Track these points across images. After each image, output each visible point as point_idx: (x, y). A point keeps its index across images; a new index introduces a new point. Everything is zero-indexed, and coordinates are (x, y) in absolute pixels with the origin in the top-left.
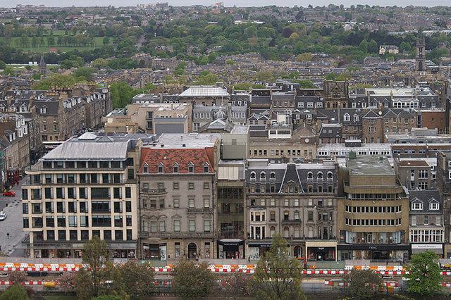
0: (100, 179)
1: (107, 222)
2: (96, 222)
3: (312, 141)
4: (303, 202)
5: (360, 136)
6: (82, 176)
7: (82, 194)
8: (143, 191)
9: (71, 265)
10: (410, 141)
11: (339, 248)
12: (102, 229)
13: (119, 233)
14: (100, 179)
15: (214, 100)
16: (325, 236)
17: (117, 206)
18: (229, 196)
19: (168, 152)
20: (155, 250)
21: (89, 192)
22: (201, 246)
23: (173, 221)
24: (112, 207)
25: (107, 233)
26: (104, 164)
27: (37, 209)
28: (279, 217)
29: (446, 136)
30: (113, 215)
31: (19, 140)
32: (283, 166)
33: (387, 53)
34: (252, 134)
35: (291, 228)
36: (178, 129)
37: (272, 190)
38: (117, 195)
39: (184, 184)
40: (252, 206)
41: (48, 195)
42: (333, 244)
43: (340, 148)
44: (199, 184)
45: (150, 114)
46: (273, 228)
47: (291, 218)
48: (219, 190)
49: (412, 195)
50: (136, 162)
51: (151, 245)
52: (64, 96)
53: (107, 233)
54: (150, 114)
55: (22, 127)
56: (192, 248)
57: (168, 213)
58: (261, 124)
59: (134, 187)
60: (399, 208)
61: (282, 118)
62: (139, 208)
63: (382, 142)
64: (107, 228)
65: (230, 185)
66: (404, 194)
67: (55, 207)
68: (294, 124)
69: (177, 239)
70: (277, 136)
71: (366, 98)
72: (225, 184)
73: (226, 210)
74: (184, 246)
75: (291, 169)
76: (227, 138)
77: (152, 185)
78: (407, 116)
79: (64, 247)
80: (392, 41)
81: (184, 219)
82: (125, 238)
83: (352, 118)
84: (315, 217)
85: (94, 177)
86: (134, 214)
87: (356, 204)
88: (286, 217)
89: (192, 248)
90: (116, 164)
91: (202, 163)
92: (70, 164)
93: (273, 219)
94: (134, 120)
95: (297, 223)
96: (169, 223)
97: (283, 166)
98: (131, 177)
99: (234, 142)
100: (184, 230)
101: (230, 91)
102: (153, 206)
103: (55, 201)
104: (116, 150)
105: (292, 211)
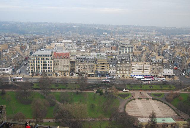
0: (45, 59)
1: (46, 68)
2: (44, 68)
3: (90, 52)
4: (88, 64)
5: (99, 51)
6: (41, 58)
7: (41, 62)
8: (54, 62)
9: (40, 77)
10: (110, 52)
11: (95, 74)
12: (45, 69)
13: (49, 70)
14: (45, 59)
15: (69, 43)
16: (92, 71)
17: (49, 64)
18: (72, 63)
19: (59, 53)
20: (56, 74)
21: (43, 61)
22: (66, 73)
23: (60, 68)
24: (48, 65)
25: (46, 70)
26: (46, 56)
27: (32, 65)
28: (83, 67)
29: (117, 52)
30: (48, 66)
31: (27, 50)
32: (84, 57)
33: (105, 34)
34: (77, 50)
35: (85, 70)
36: (62, 49)
38: (49, 62)
39: (63, 60)
40: (77, 65)
41: (34, 62)
42: (94, 73)
43: (95, 54)
44: (66, 60)
45: (56, 45)
46: (81, 70)
47: (85, 68)
48: (70, 62)
49: (110, 63)
50: (53, 55)
51: (56, 73)
52: (37, 41)
53: (46, 70)
54: (56, 45)
55: (28, 48)
56: (64, 74)
57: (59, 66)
58: (79, 48)
59: (52, 61)
60: (107, 66)
61: (83, 47)
62: (53, 65)
63: (104, 52)
64: (47, 69)
65: (73, 61)
66: (108, 63)
67: (35, 65)
69: (61, 71)
70: (82, 51)
71: (101, 43)
72: (71, 60)
73: (71, 66)
74: (63, 73)
75: (85, 58)
76: (72, 51)
79: (37, 73)
80: (105, 31)
81: (63, 68)
82: (50, 71)
83: (98, 47)
84: (90, 68)
85: (44, 58)
86: (52, 66)
87: (98, 65)
88: (84, 68)
89: (64, 74)
90: (48, 56)
91: (67, 56)
92: (39, 56)
93: (81, 68)
94: (52, 46)
96: (60, 68)
97: (84, 57)
98: (52, 59)
99: (74, 52)
100: (63, 70)
101: (72, 41)
102: (56, 65)
103: (35, 63)
104: (49, 53)
105: (85, 66)
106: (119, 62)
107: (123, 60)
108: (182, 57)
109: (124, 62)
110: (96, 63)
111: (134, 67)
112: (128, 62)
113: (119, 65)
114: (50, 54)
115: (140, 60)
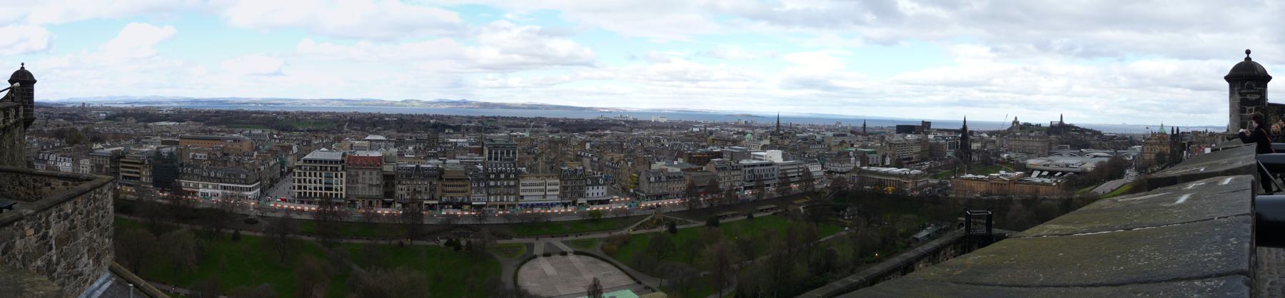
16: (433, 198)
18: (389, 179)
22: (374, 202)
23: (362, 190)
26: (331, 162)
28: (412, 189)
37: (409, 176)
44: (375, 173)
56: (370, 203)
57: (360, 186)
61: (410, 148)
68: (416, 151)
69: (363, 198)
73: (386, 185)
74: (367, 202)
77: (353, 172)
78: (465, 149)
89: (370, 203)
90: (336, 162)
95: (420, 192)
104: (337, 156)
106: (492, 176)
107: (501, 172)
108: (618, 163)
109: (502, 176)
110: (441, 179)
111: (524, 185)
112: (512, 176)
113: (492, 183)
114: (340, 158)
115: (533, 170)
